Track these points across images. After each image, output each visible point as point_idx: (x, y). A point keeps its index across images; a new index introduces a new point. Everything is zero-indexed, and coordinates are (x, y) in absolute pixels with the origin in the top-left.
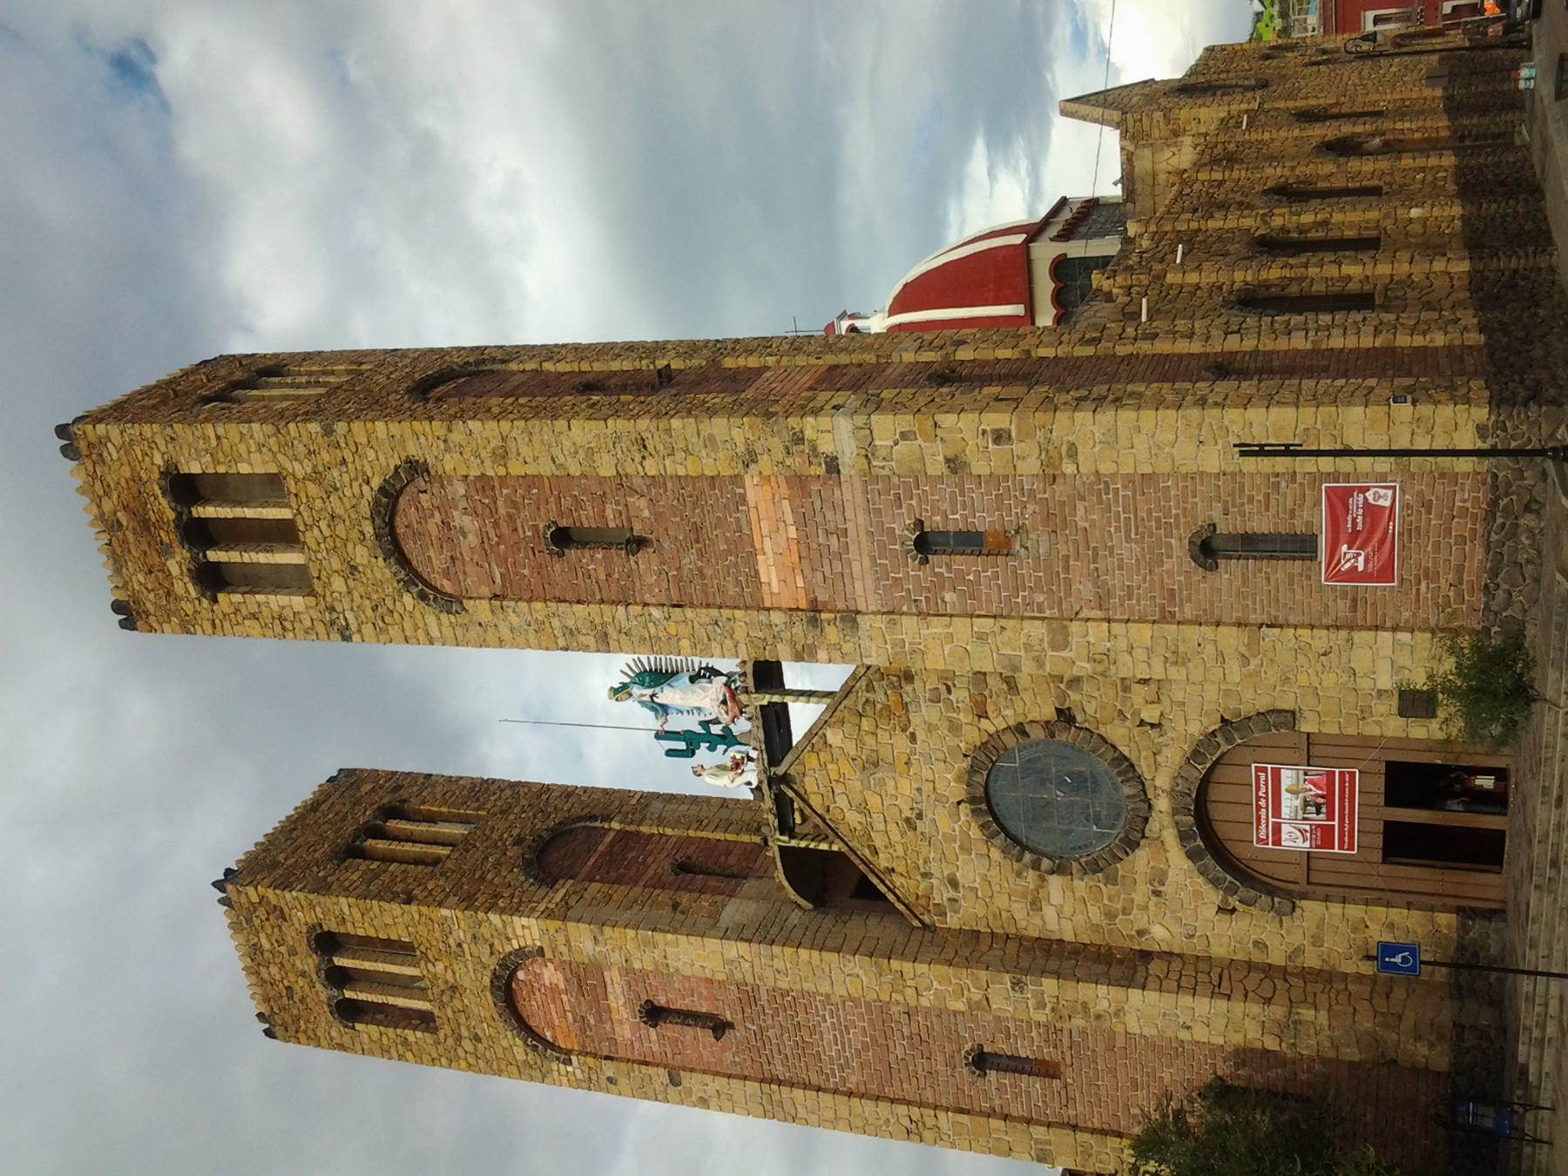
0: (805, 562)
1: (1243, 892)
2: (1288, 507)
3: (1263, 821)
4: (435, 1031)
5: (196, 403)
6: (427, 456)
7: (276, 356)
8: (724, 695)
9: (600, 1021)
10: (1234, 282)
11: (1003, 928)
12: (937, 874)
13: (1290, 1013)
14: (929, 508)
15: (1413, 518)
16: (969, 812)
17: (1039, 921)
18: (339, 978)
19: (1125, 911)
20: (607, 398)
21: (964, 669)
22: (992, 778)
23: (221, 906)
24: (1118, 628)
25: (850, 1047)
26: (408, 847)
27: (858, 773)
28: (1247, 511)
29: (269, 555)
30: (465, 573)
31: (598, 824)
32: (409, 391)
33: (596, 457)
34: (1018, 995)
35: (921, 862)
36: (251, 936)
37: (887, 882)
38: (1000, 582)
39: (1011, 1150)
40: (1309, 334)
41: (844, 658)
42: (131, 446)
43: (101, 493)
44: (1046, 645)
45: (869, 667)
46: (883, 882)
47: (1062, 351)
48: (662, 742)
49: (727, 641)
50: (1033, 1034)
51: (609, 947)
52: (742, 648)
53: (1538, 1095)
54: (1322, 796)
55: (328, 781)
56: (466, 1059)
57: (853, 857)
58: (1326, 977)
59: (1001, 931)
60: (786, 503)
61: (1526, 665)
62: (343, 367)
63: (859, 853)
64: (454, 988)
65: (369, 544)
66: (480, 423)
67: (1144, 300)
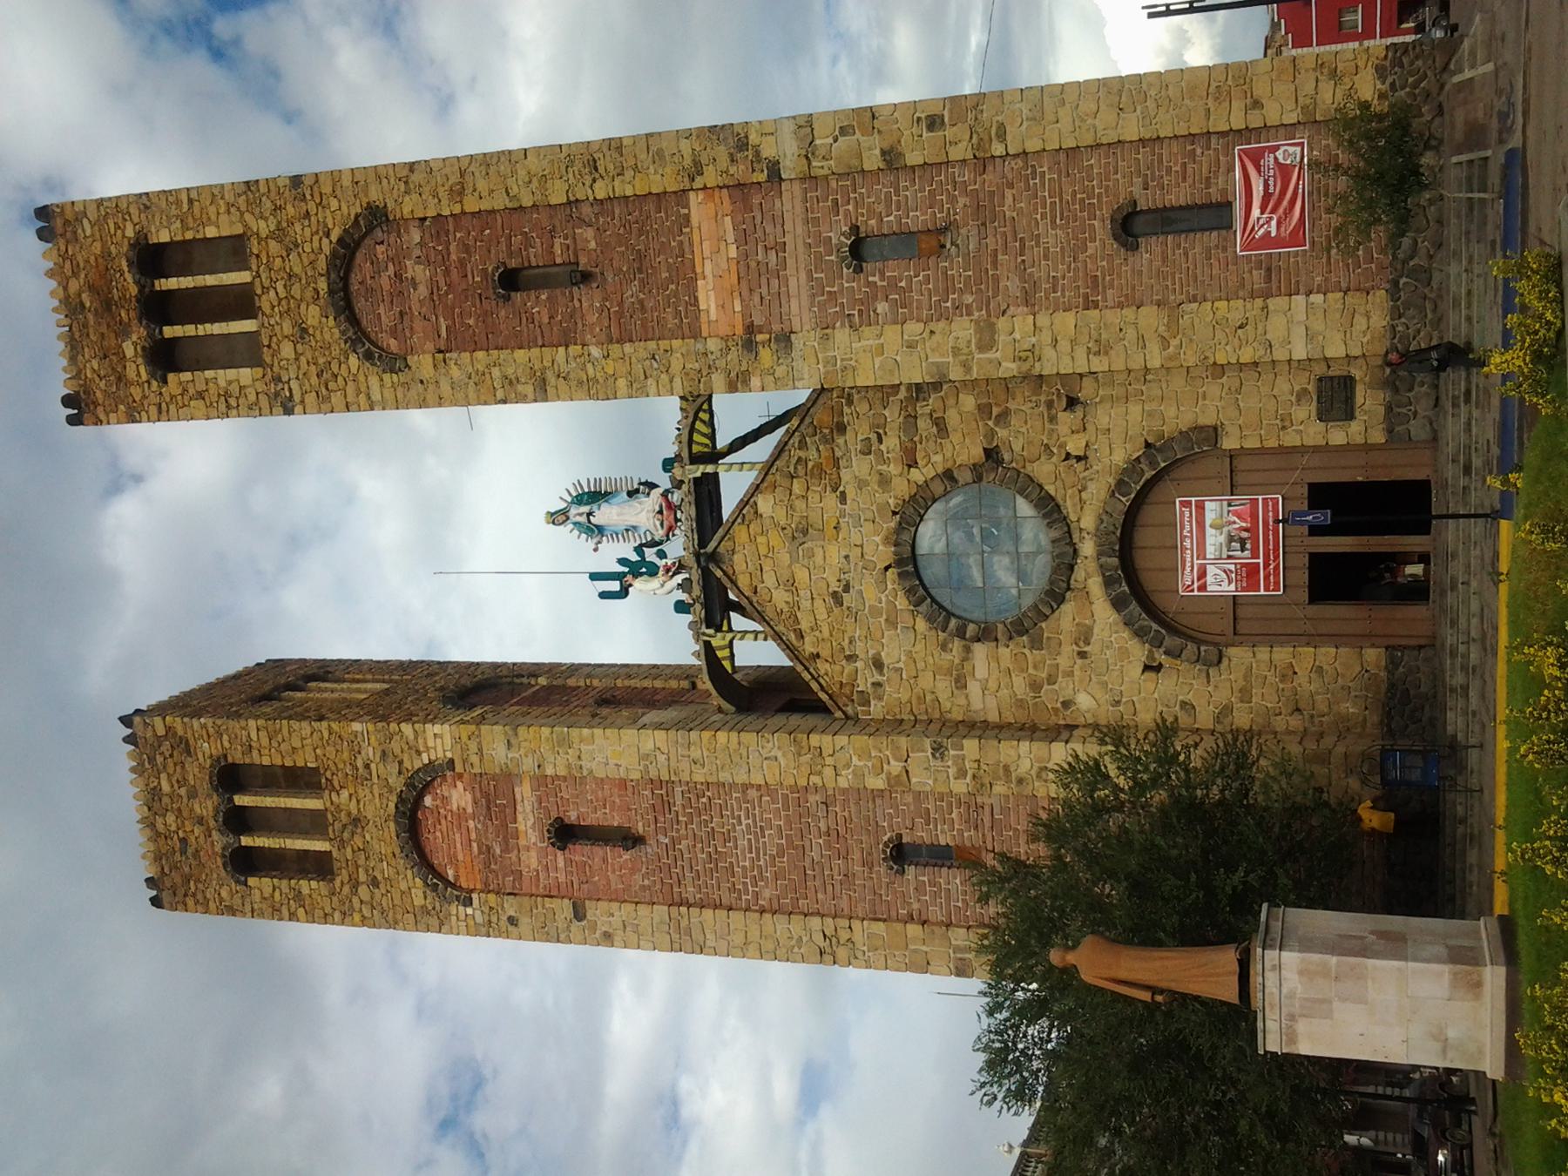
0: (744, 283)
1: (1171, 641)
3: (1188, 564)
6: (387, 200)
8: (661, 506)
9: (506, 849)
14: (864, 211)
17: (963, 701)
18: (238, 821)
19: (1051, 680)
25: (765, 854)
27: (787, 544)
28: (1166, 182)
29: (224, 324)
31: (525, 680)
34: (939, 763)
36: (152, 779)
37: (812, 670)
39: (928, 963)
43: (70, 274)
44: (973, 346)
48: (595, 582)
49: (664, 376)
50: (954, 815)
51: (522, 751)
52: (677, 382)
54: (1246, 530)
60: (728, 220)
64: (356, 821)
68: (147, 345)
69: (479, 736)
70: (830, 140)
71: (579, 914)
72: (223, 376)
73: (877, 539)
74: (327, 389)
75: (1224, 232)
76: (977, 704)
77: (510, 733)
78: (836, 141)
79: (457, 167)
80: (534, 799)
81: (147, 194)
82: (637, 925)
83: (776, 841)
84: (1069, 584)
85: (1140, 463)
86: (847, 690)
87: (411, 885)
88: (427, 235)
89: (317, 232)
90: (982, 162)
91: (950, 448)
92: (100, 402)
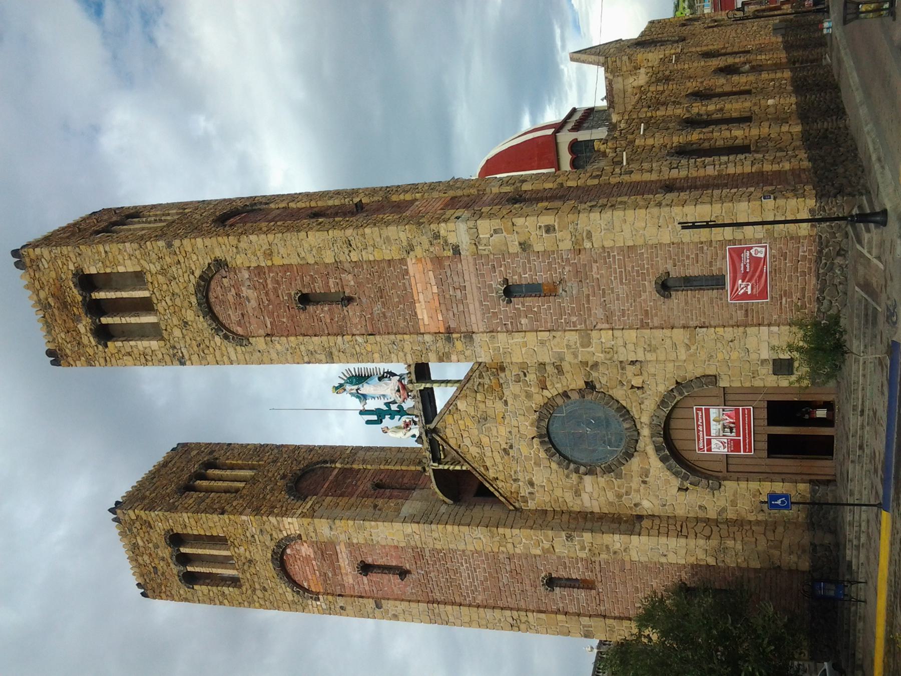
0: (443, 306)
1: (692, 478)
3: (701, 438)
4: (240, 587)
5: (91, 234)
7: (135, 207)
8: (398, 387)
9: (335, 574)
10: (673, 143)
11: (560, 507)
12: (522, 479)
13: (721, 543)
15: (777, 263)
17: (579, 502)
18: (183, 560)
19: (627, 493)
20: (328, 220)
21: (532, 361)
22: (551, 422)
23: (114, 523)
24: (618, 333)
25: (477, 580)
26: (220, 483)
28: (686, 263)
29: (137, 318)
30: (250, 323)
31: (328, 465)
32: (214, 221)
33: (323, 252)
34: (570, 543)
35: (512, 473)
37: (494, 485)
38: (551, 311)
40: (716, 167)
41: (467, 359)
42: (55, 260)
45: (480, 364)
46: (492, 485)
47: (580, 183)
50: (579, 565)
53: (858, 576)
54: (733, 423)
55: (172, 450)
56: (259, 602)
57: (474, 473)
58: (739, 523)
59: (559, 509)
60: (431, 273)
61: (841, 333)
62: (174, 211)
63: (478, 470)
64: (250, 561)
65: (194, 309)
66: (256, 236)
67: (624, 153)
68: (93, 328)
69: (314, 524)
72: (142, 345)
77: (331, 523)
82: (411, 612)
83: (483, 574)
84: (635, 449)
87: (285, 590)
88: (253, 275)
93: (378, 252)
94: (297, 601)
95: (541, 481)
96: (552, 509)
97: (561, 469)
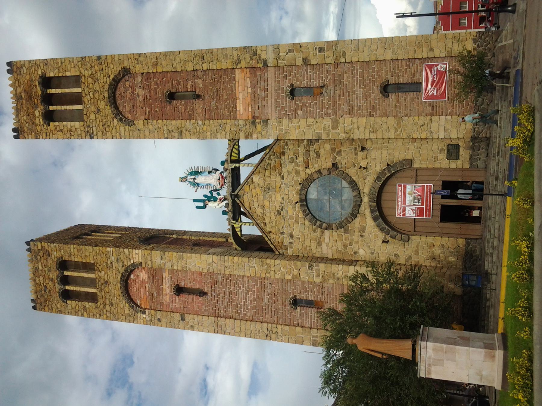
1: (392, 233)
2: (412, 73)
3: (400, 207)
6: (130, 66)
8: (219, 177)
14: (296, 79)
16: (299, 206)
18: (65, 280)
19: (351, 244)
25: (249, 300)
28: (399, 75)
29: (71, 106)
31: (168, 236)
34: (311, 271)
37: (268, 237)
38: (317, 106)
39: (303, 341)
44: (330, 128)
49: (223, 133)
50: (315, 290)
51: (166, 261)
52: (228, 135)
54: (420, 196)
56: (106, 314)
60: (248, 79)
63: (260, 225)
64: (107, 282)
65: (105, 100)
68: (44, 112)
70: (285, 54)
71: (183, 319)
72: (69, 124)
73: (294, 192)
74: (106, 131)
75: (418, 93)
76: (325, 251)
77: (162, 254)
78: (287, 54)
79: (155, 56)
80: (169, 277)
81: (47, 59)
83: (253, 296)
85: (385, 171)
86: (280, 244)
89: (105, 76)
90: (337, 64)
91: (321, 162)
92: (26, 131)
93: (219, 64)
94: (131, 314)
95: (298, 234)
96: (302, 255)
97: (311, 226)
